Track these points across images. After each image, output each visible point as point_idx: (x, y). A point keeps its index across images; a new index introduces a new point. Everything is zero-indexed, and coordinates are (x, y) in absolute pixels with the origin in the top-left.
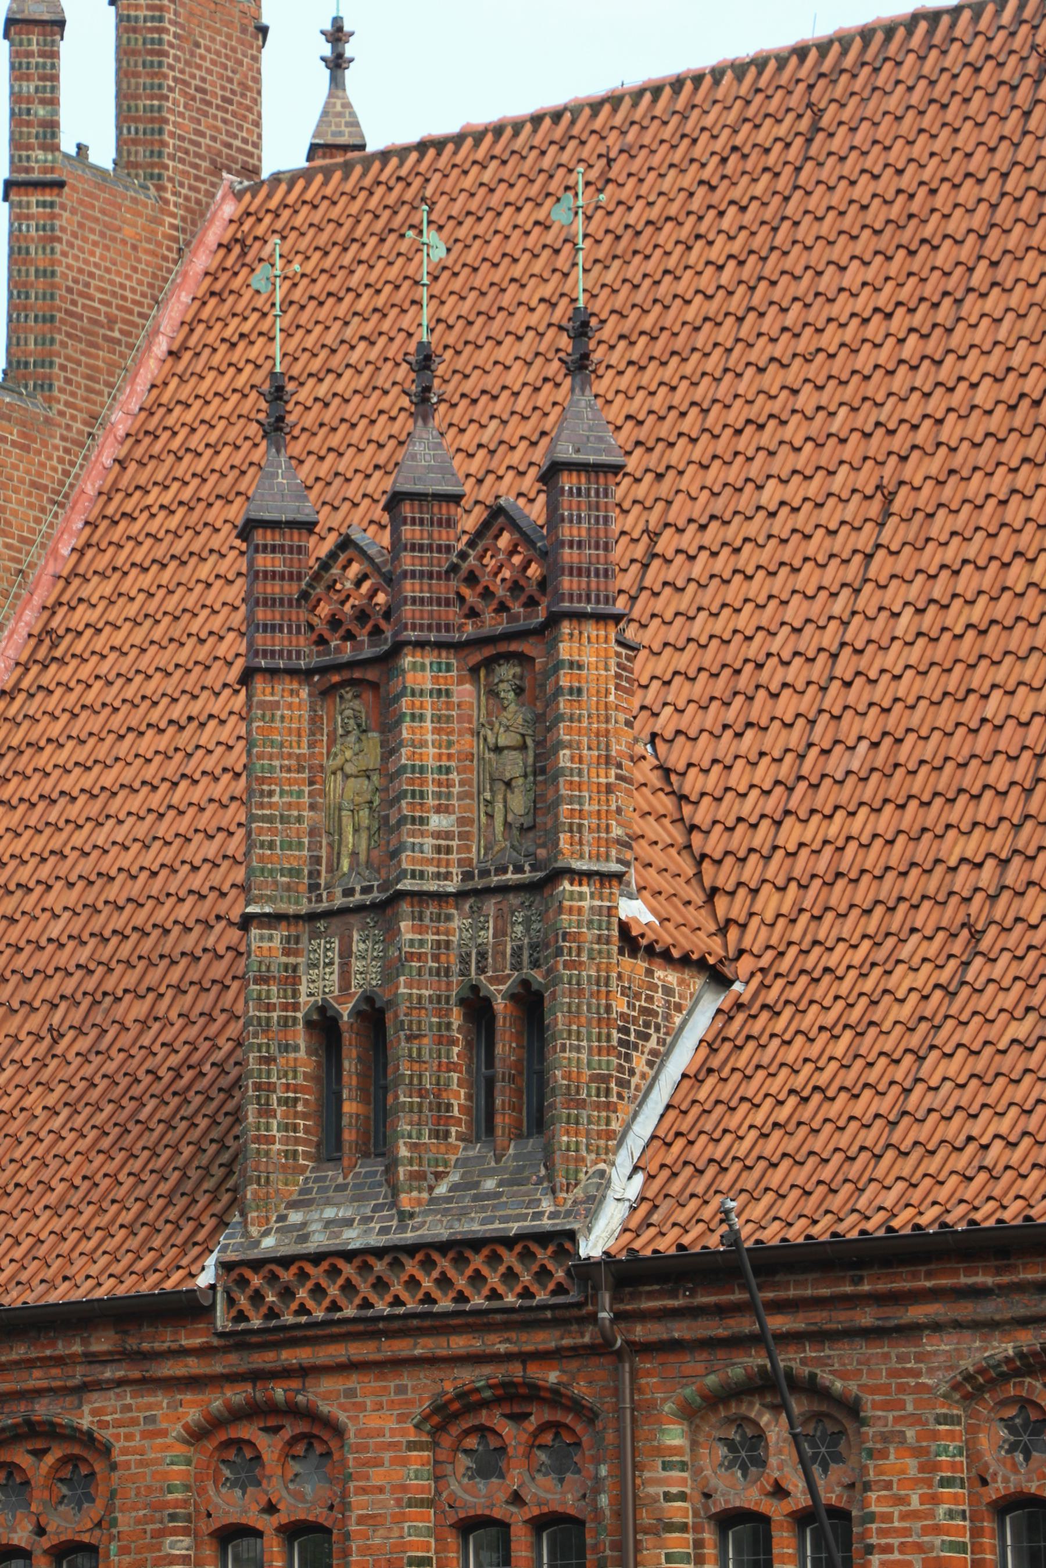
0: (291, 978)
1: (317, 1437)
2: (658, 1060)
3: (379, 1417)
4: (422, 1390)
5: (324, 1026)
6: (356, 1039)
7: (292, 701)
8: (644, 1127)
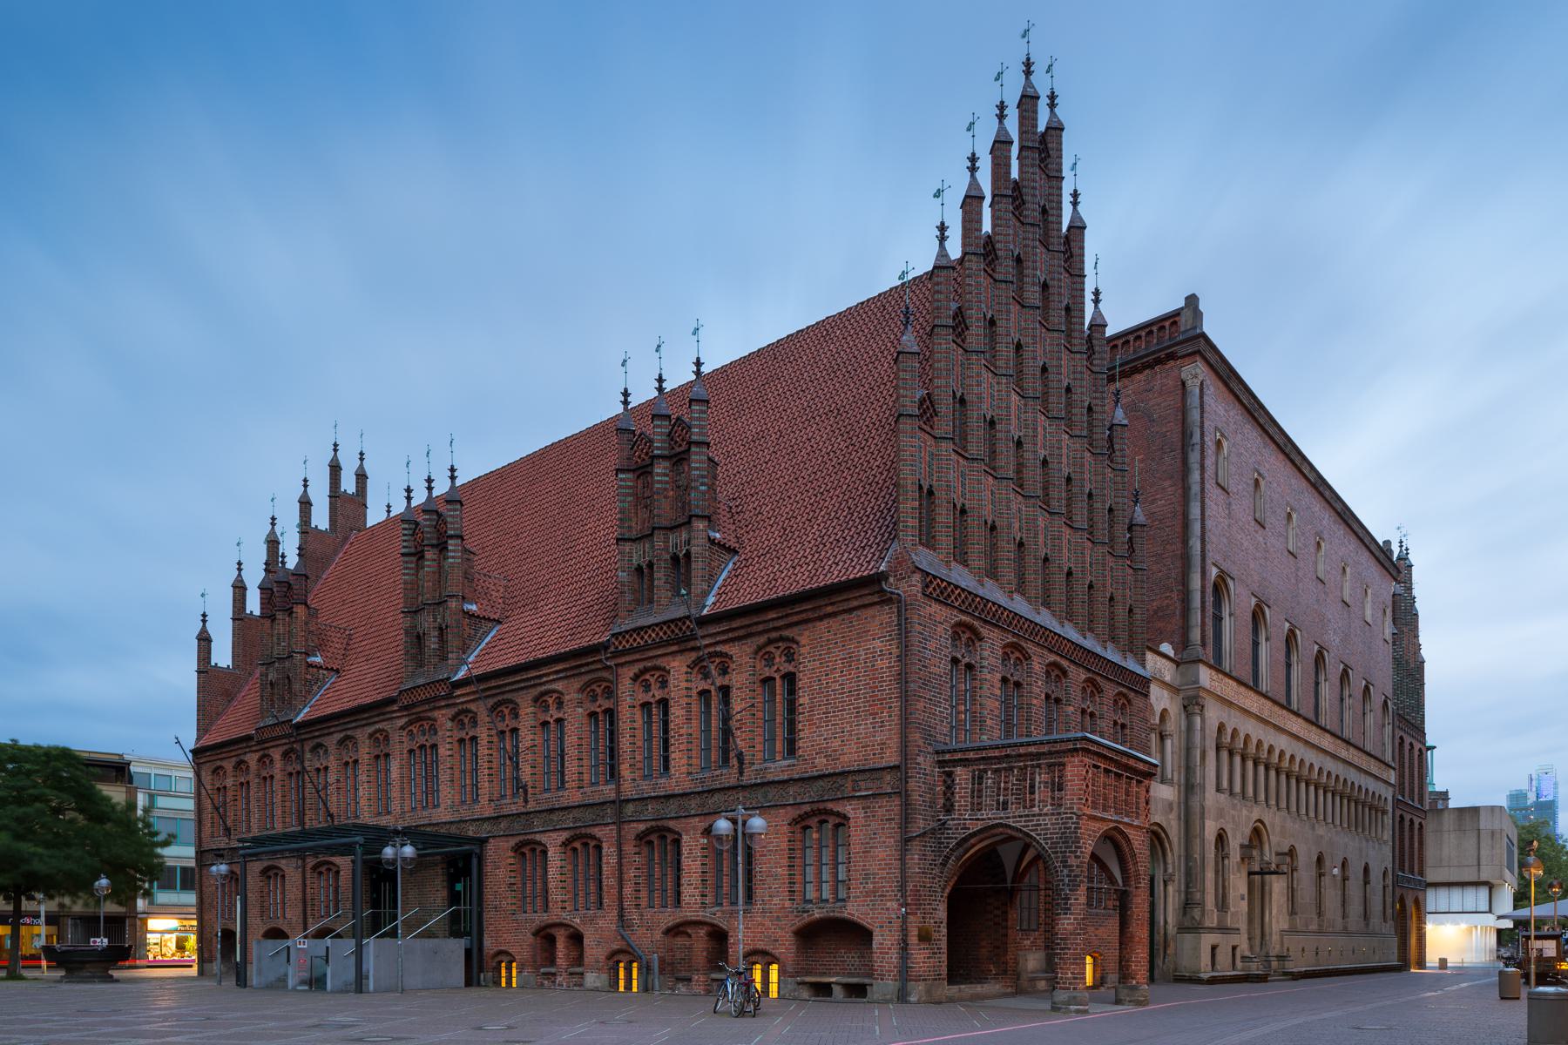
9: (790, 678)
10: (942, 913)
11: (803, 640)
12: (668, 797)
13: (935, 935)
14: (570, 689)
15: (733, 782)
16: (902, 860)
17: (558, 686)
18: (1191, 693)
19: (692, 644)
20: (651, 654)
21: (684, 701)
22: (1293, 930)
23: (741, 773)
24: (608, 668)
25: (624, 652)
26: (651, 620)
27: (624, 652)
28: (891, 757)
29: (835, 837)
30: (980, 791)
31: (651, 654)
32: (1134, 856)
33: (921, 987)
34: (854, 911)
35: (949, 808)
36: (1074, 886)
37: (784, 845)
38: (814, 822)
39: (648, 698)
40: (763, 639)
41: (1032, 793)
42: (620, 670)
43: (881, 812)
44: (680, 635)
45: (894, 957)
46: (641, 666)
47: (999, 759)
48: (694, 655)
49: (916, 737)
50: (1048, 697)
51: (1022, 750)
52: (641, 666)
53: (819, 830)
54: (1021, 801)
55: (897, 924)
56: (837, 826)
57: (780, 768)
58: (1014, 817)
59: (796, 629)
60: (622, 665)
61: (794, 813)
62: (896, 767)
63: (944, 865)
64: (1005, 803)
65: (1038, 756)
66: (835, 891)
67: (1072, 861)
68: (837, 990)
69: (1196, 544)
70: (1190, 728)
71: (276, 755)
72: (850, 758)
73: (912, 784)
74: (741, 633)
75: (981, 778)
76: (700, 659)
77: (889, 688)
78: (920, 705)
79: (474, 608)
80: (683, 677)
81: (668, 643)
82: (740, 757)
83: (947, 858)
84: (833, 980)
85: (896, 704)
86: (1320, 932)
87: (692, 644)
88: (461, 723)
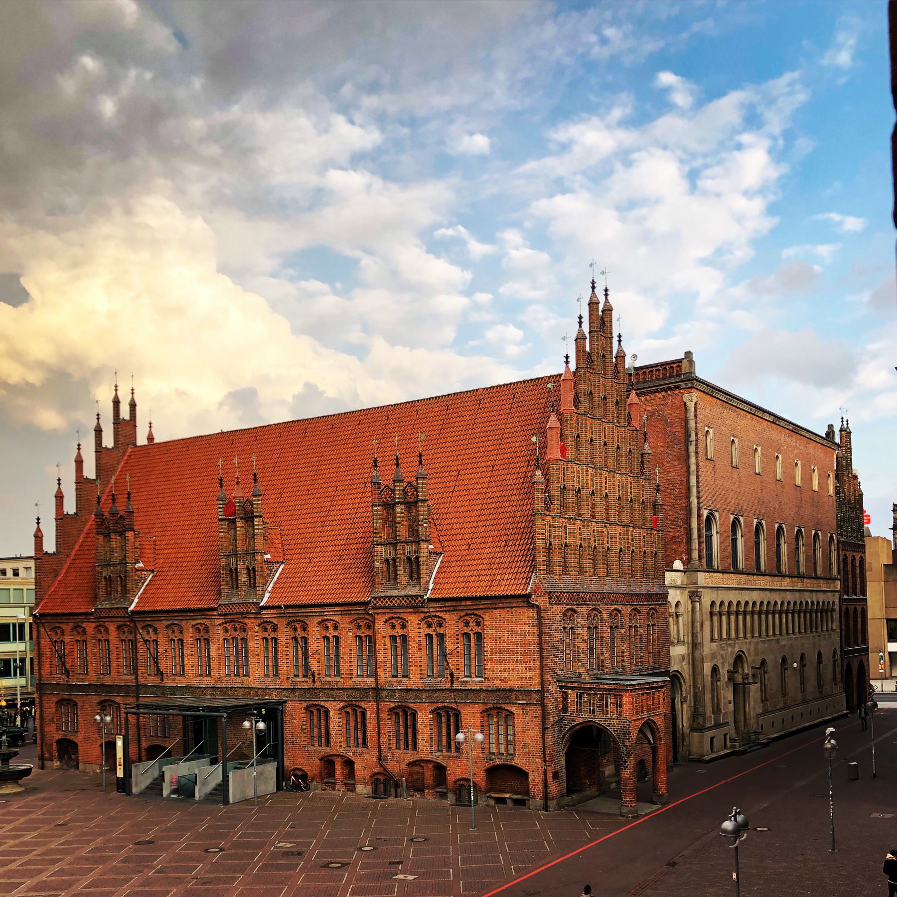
0: (101, 573)
1: (107, 630)
2: (143, 584)
3: (112, 628)
4: (116, 624)
5: (105, 578)
6: (109, 580)
7: (101, 538)
8: (139, 594)
9: (479, 636)
10: (563, 762)
11: (486, 617)
12: (408, 690)
13: (560, 774)
14: (345, 622)
15: (448, 686)
16: (543, 738)
17: (337, 618)
18: (693, 589)
19: (423, 610)
20: (397, 611)
21: (417, 639)
22: (765, 712)
23: (452, 682)
24: (369, 614)
25: (380, 608)
26: (395, 593)
27: (380, 608)
28: (537, 687)
29: (506, 721)
30: (581, 703)
31: (397, 611)
32: (658, 729)
33: (555, 802)
34: (518, 762)
35: (565, 709)
36: (629, 756)
37: (478, 724)
38: (494, 712)
39: (394, 633)
40: (463, 614)
41: (607, 707)
42: (376, 616)
43: (531, 713)
44: (416, 604)
45: (540, 787)
46: (390, 615)
47: (590, 689)
48: (423, 615)
49: (548, 676)
50: (611, 627)
51: (601, 686)
52: (390, 615)
53: (497, 716)
54: (601, 711)
55: (541, 771)
56: (507, 716)
57: (474, 682)
58: (598, 719)
59: (481, 611)
60: (378, 614)
61: (482, 707)
62: (538, 691)
63: (563, 738)
64: (594, 710)
65: (609, 690)
66: (507, 749)
67: (627, 743)
68: (509, 802)
69: (694, 500)
70: (693, 609)
71: (112, 628)
72: (514, 683)
73: (546, 700)
74: (451, 609)
75: (581, 697)
76: (426, 618)
77: (534, 651)
78: (549, 660)
79: (269, 556)
80: (416, 626)
81: (407, 607)
82: (452, 675)
83: (565, 735)
84: (507, 796)
85: (538, 659)
86: (786, 707)
87: (423, 610)
88: (266, 630)
